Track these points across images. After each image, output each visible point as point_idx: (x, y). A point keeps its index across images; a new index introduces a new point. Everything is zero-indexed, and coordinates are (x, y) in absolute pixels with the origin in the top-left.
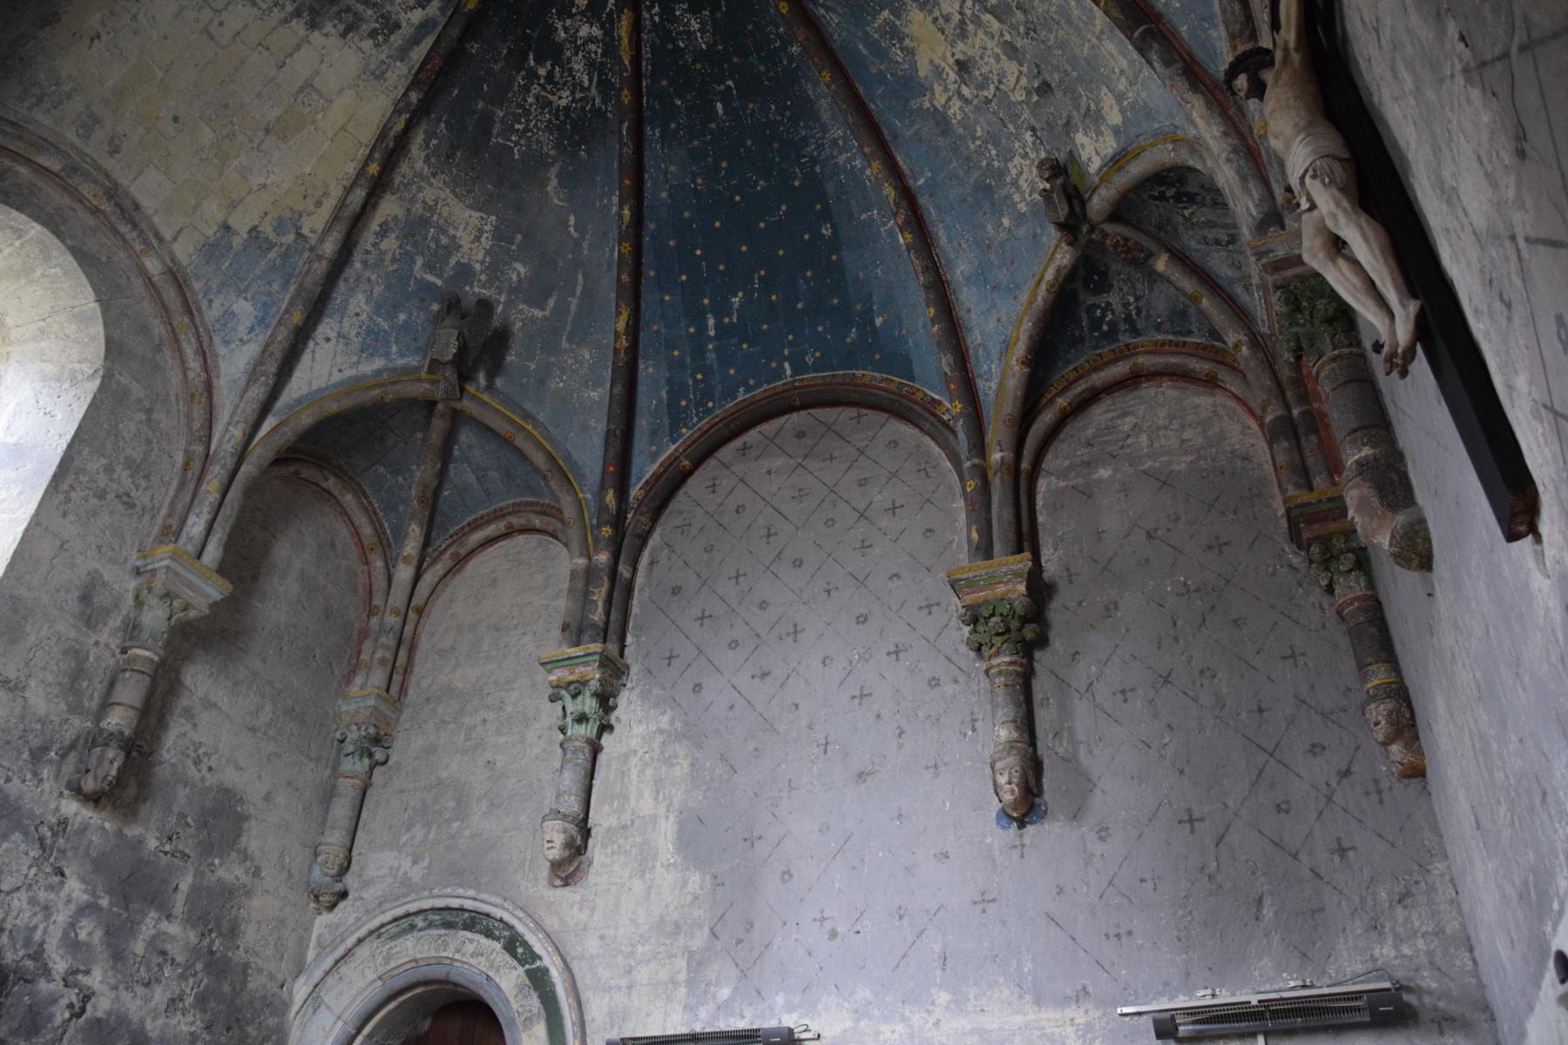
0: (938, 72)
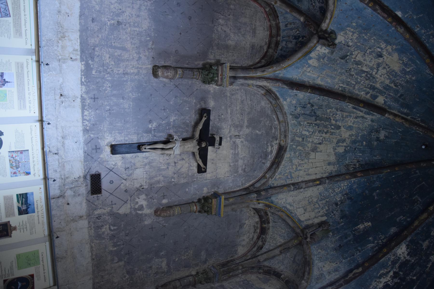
0: (389, 54)
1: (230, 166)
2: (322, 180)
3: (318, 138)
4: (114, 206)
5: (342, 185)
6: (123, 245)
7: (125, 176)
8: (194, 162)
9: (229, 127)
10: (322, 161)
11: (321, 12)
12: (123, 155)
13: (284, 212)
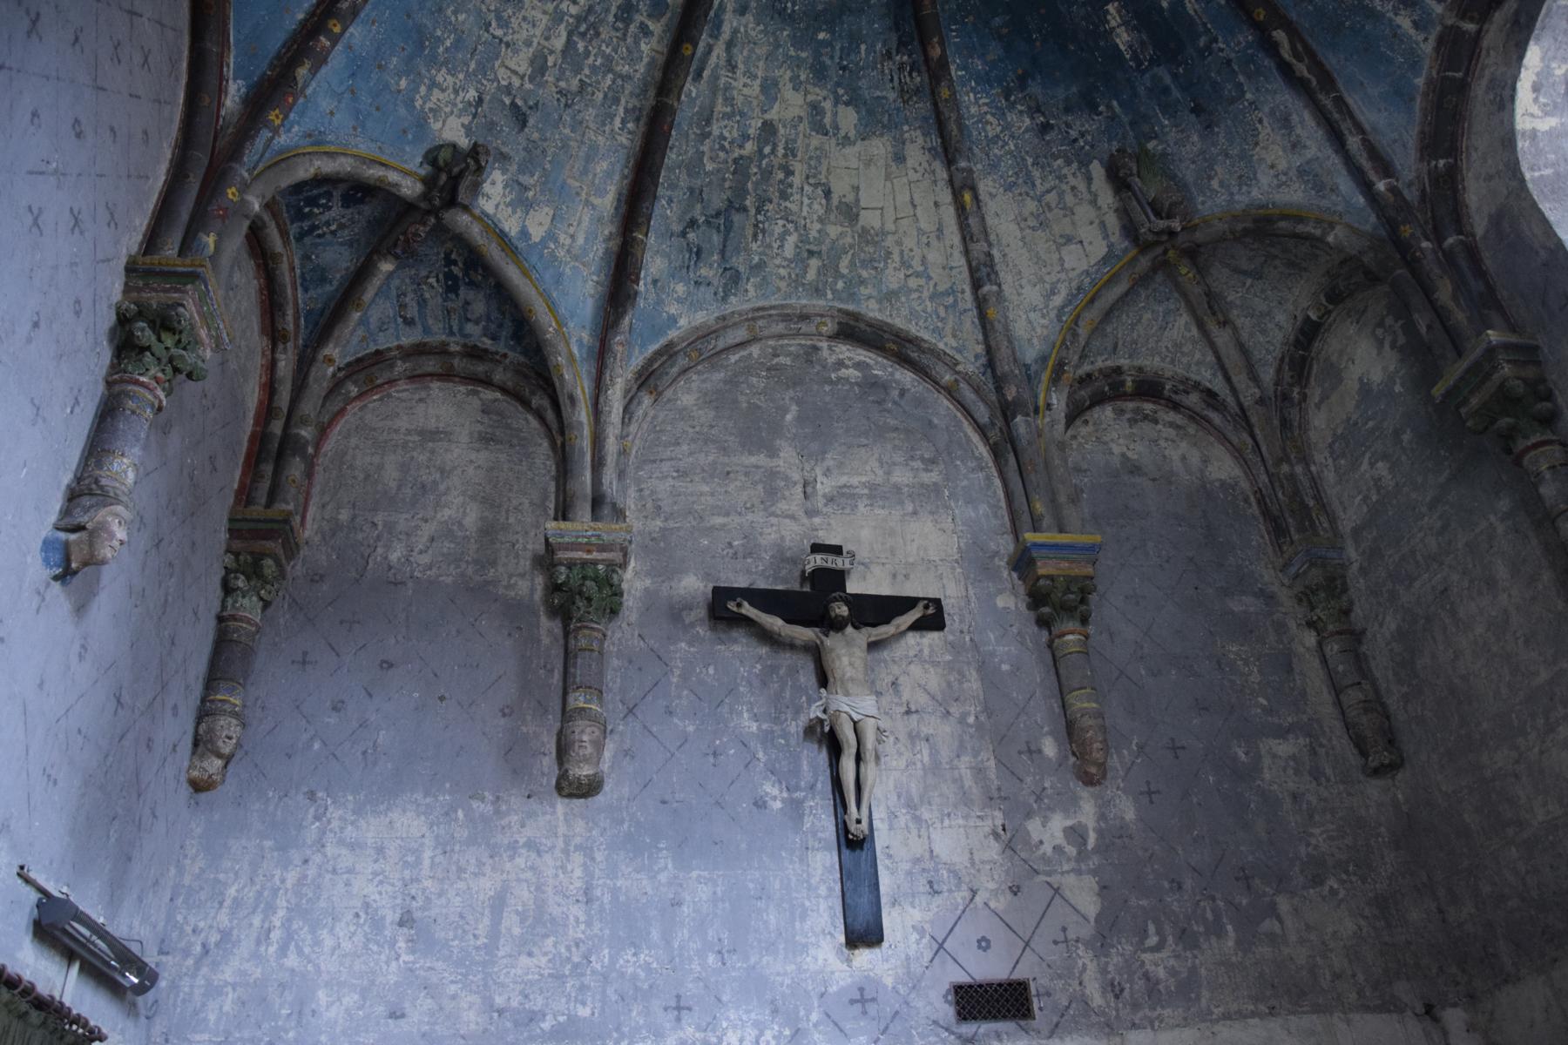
1: (915, 513)
2: (957, 184)
3: (806, 201)
4: (1071, 935)
5: (973, 110)
6: (1213, 899)
7: (961, 896)
8: (903, 642)
9: (774, 520)
10: (888, 184)
11: (361, 201)
12: (883, 901)
13: (1078, 316)
